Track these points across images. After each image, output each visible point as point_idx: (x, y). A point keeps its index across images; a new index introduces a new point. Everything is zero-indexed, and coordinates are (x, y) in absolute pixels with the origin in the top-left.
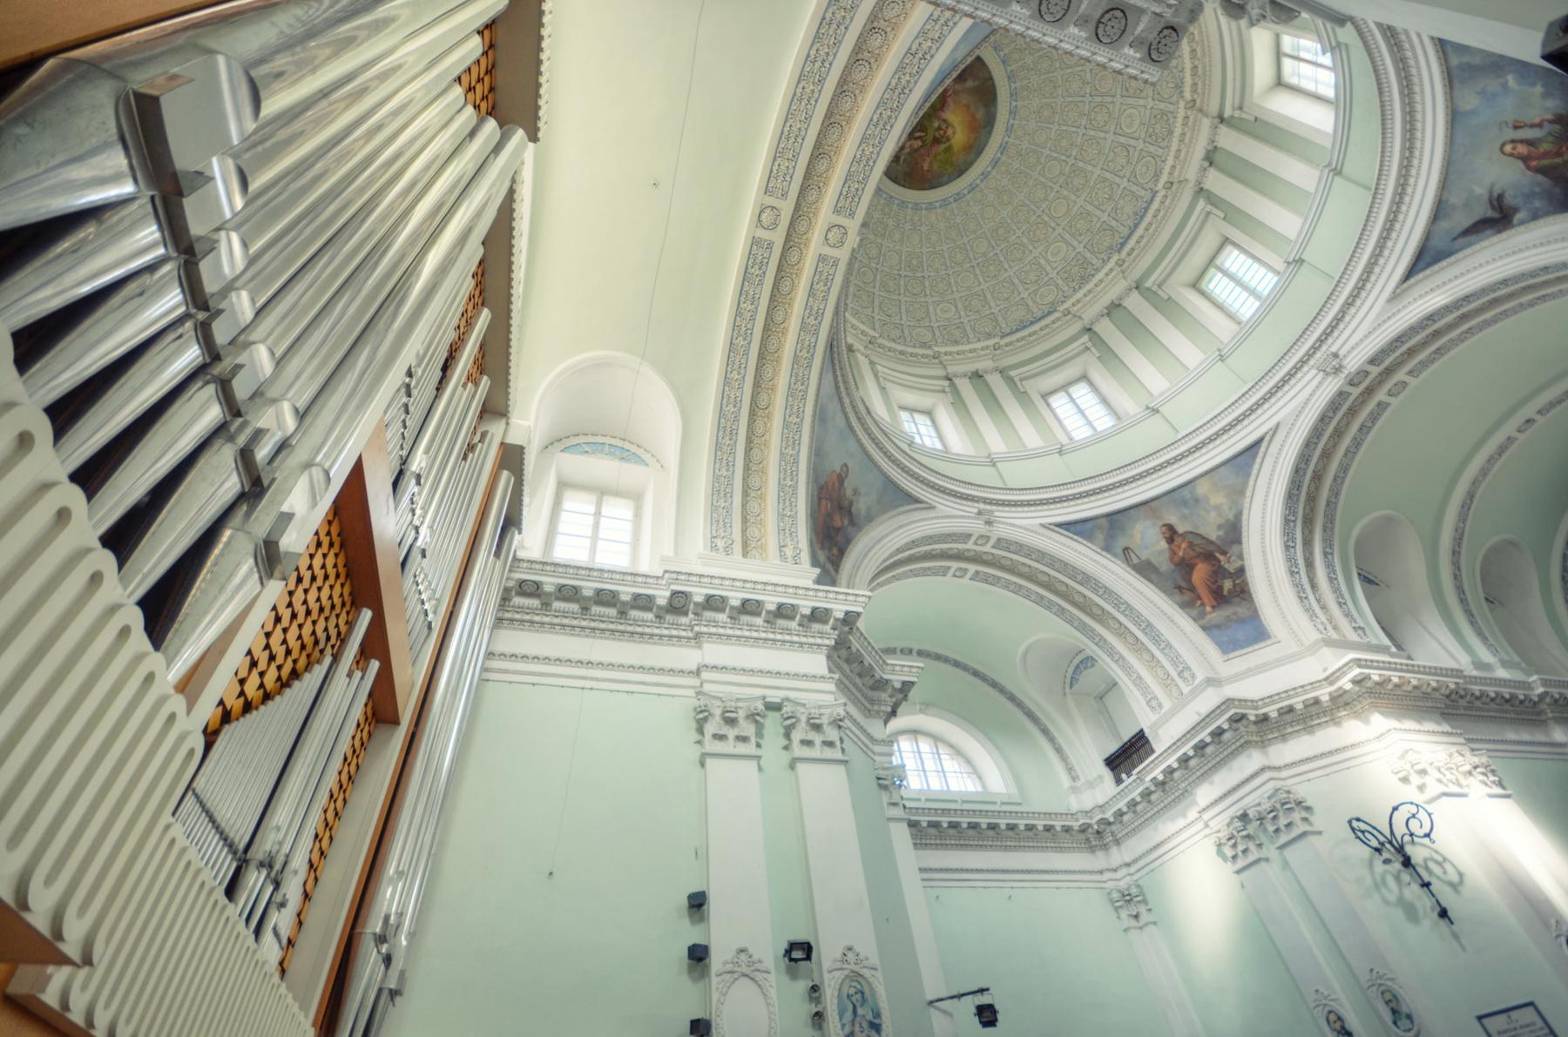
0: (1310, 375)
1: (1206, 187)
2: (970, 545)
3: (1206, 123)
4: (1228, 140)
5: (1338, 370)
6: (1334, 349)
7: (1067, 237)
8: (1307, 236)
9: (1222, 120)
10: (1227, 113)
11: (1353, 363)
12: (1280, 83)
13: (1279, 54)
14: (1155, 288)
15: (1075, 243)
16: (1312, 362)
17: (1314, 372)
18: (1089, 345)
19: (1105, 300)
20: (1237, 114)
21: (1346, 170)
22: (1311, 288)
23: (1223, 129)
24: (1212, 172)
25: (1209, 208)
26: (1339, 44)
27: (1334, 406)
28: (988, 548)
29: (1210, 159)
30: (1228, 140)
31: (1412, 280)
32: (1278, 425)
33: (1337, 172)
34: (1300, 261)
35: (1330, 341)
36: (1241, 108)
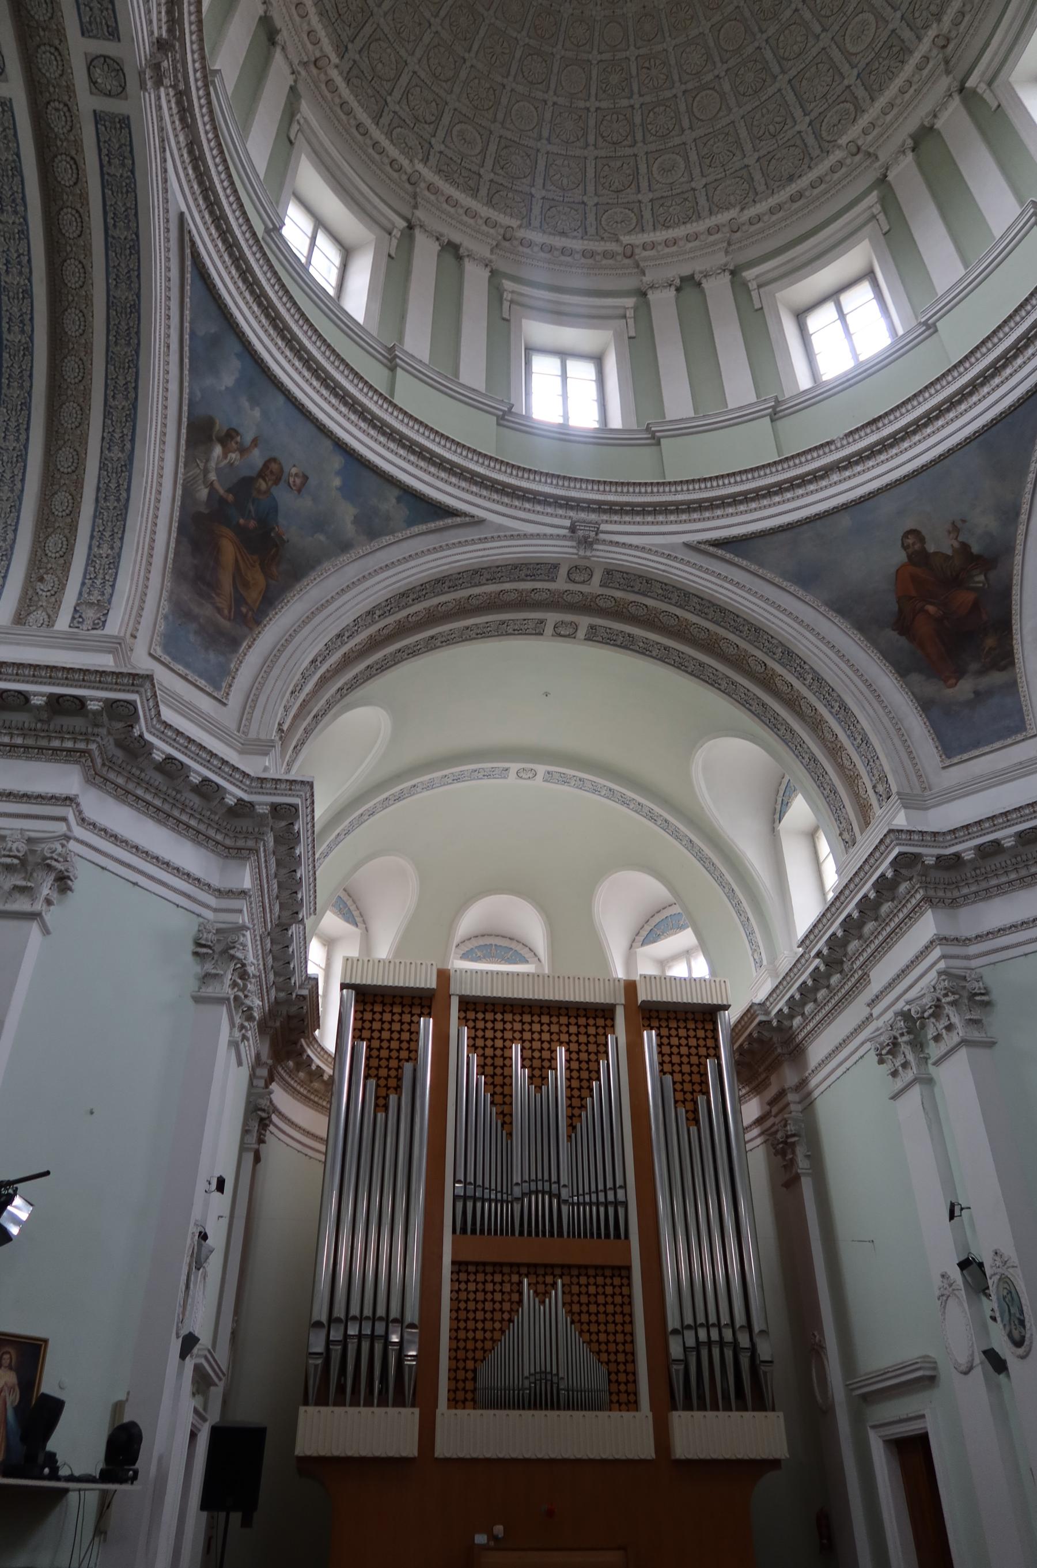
0: (562, 520)
1: (651, 296)
2: (79, 48)
3: (721, 259)
4: (718, 290)
5: (586, 543)
6: (604, 527)
7: (492, 148)
8: (683, 430)
9: (733, 273)
10: (749, 274)
11: (604, 555)
12: (800, 316)
13: (834, 295)
14: (507, 296)
15: (489, 162)
16: (571, 514)
17: (567, 523)
18: (396, 233)
19: (457, 238)
20: (753, 285)
21: (779, 423)
22: (639, 466)
23: (727, 277)
24: (672, 293)
25: (630, 313)
26: (934, 324)
27: (548, 569)
28: (87, 102)
29: (689, 284)
30: (718, 290)
31: (720, 552)
32: (481, 521)
33: (775, 415)
34: (655, 440)
35: (605, 517)
36: (759, 286)
